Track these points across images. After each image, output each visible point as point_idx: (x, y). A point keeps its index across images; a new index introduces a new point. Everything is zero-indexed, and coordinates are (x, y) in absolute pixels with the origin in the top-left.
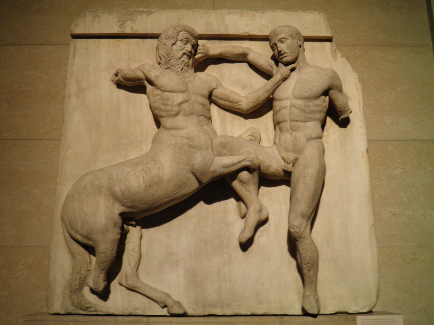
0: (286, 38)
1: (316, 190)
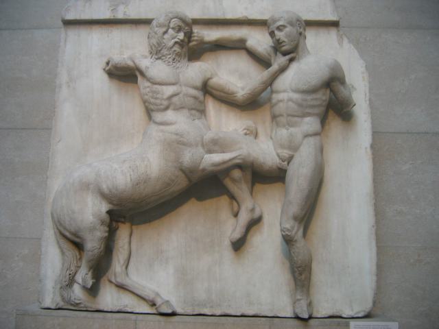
0: (284, 26)
1: (310, 191)
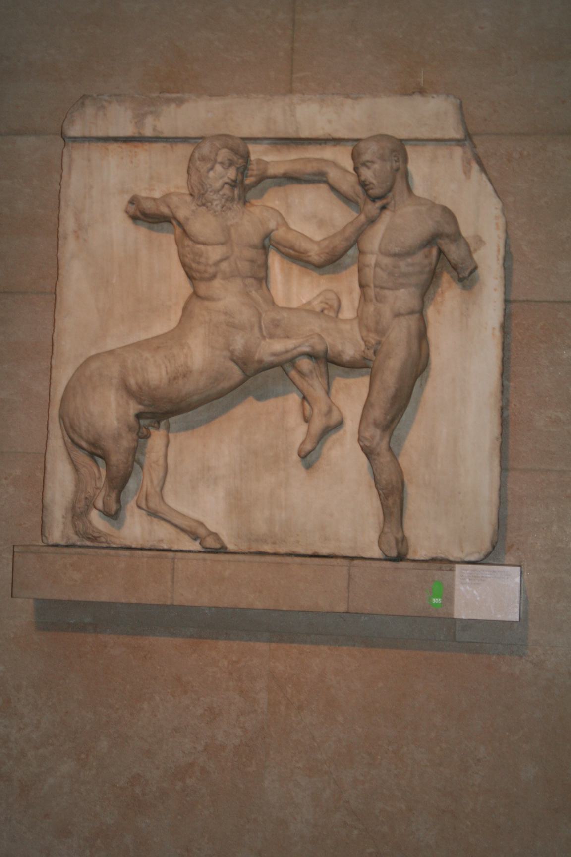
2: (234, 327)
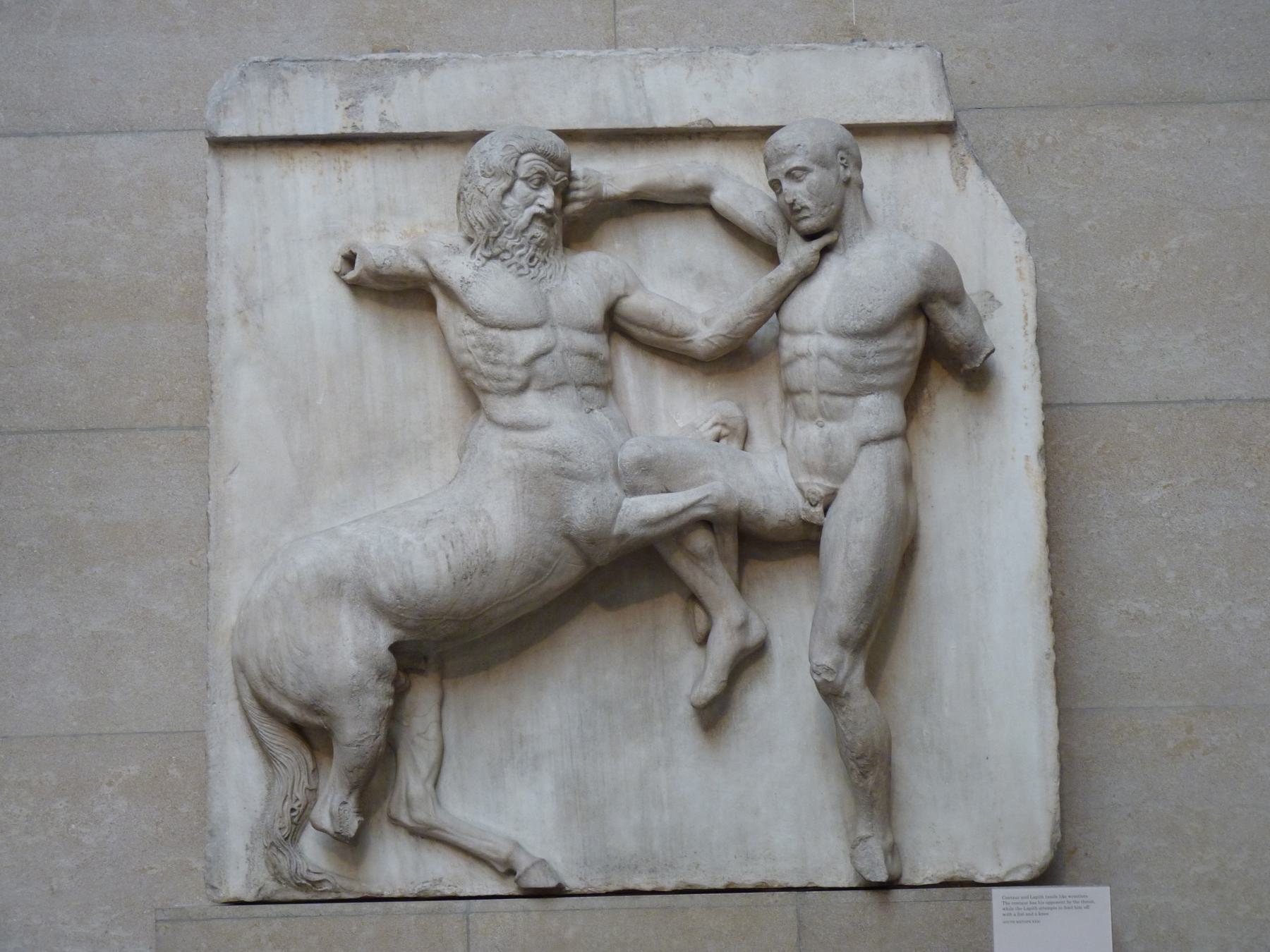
0: (805, 170)
1: (878, 577)
2: (571, 478)
